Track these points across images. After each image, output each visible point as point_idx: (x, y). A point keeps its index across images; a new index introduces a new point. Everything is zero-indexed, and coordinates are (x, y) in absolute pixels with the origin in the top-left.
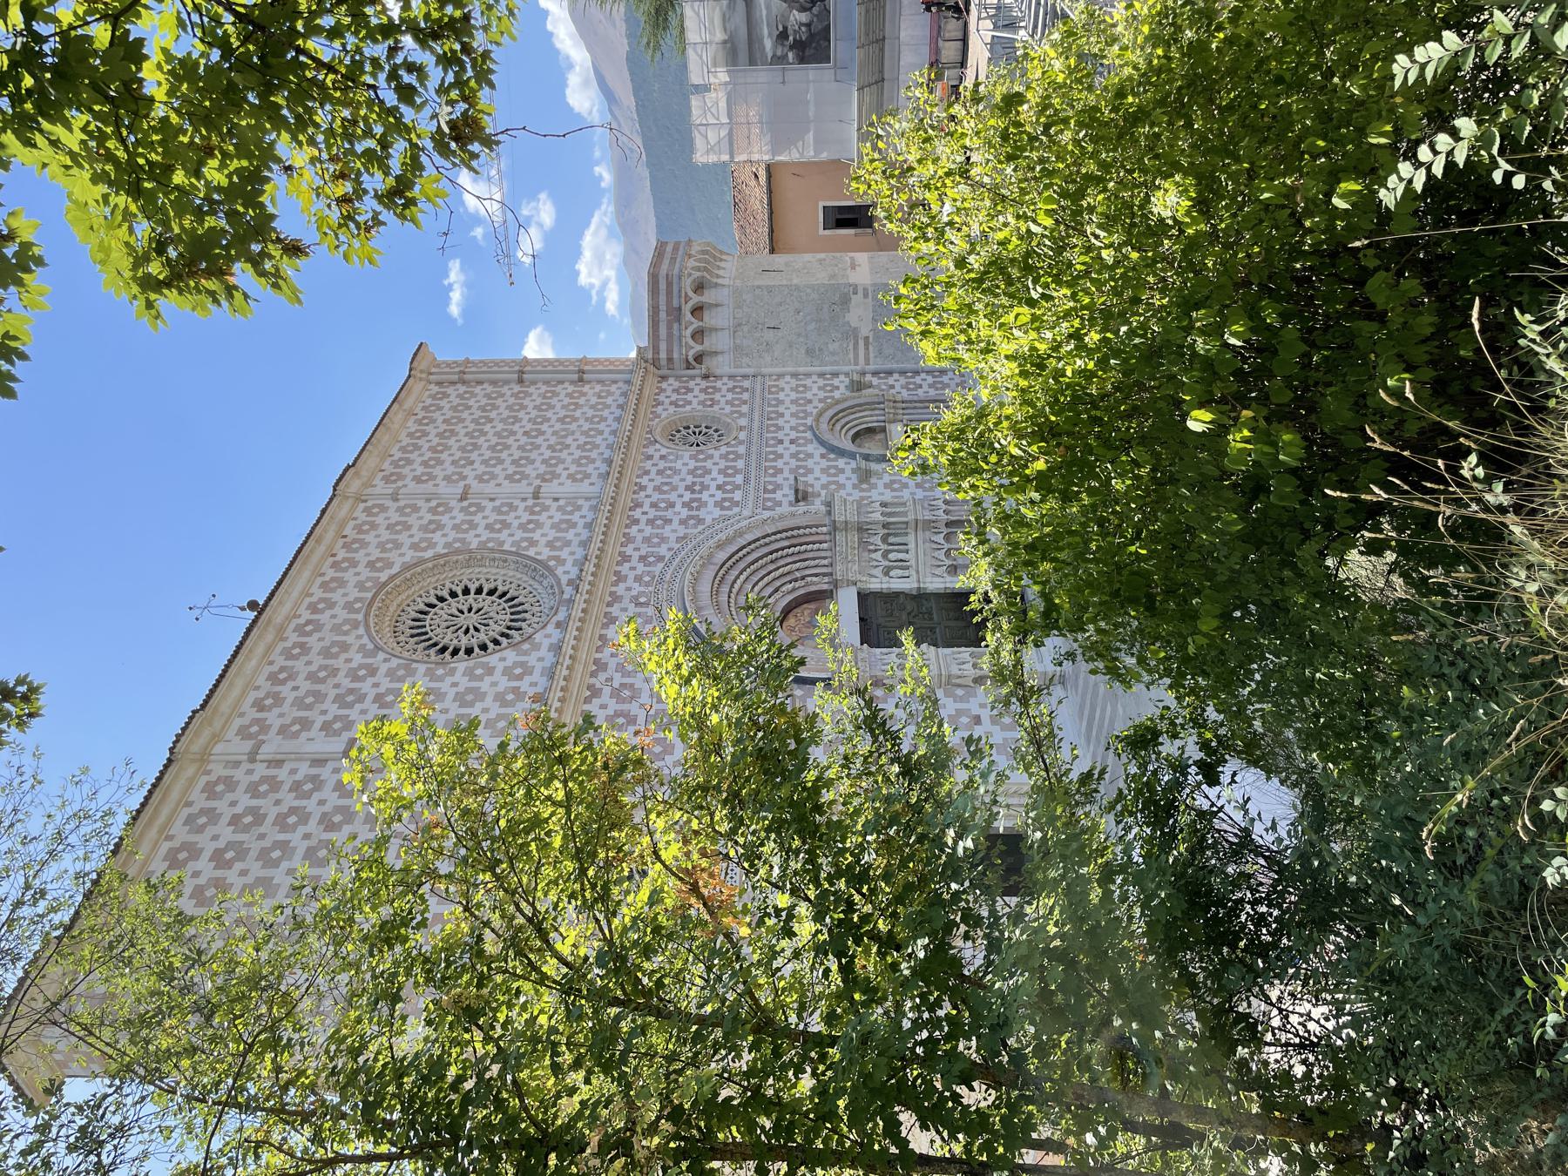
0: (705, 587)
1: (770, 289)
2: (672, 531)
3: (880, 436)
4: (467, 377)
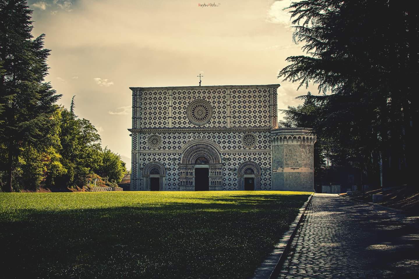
0: (201, 146)
1: (283, 152)
2: (217, 140)
3: (252, 173)
4: (271, 95)
